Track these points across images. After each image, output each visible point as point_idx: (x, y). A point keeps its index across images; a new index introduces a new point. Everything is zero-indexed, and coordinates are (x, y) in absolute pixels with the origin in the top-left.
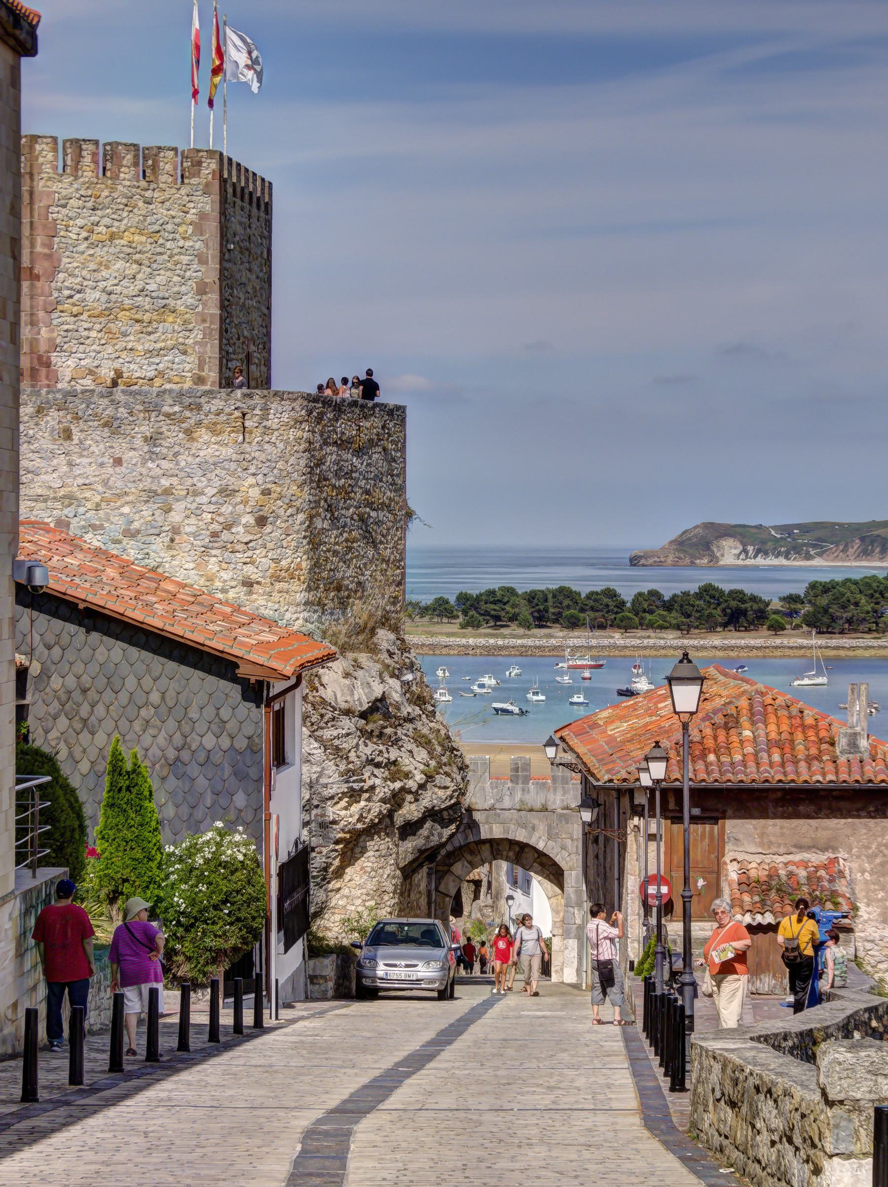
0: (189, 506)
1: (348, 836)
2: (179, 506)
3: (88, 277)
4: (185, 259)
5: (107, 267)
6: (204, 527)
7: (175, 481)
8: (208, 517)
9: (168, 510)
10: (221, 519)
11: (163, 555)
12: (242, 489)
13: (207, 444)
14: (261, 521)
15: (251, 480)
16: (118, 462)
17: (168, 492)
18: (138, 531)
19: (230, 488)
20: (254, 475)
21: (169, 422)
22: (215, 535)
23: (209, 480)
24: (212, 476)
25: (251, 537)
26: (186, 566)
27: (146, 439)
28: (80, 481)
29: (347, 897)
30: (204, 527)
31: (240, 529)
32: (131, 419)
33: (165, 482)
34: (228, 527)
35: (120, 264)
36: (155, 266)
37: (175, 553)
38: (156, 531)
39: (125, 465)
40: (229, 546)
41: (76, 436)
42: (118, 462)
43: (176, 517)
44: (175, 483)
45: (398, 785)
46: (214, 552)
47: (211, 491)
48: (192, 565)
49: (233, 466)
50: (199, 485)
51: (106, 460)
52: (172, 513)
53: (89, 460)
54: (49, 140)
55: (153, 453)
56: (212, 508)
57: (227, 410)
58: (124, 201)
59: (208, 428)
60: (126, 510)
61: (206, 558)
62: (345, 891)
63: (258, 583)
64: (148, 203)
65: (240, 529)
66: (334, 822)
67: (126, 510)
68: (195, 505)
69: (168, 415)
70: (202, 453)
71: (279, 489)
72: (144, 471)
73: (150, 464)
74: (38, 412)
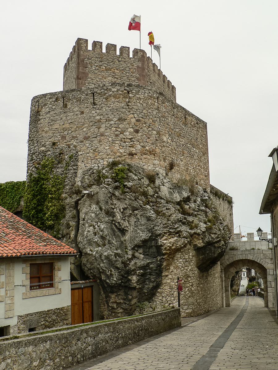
0: (107, 125)
1: (168, 252)
2: (103, 126)
3: (99, 80)
4: (133, 79)
5: (105, 78)
6: (113, 132)
7: (102, 117)
8: (114, 129)
9: (99, 128)
10: (119, 130)
11: (97, 145)
12: (128, 119)
13: (114, 103)
14: (137, 131)
15: (132, 116)
16: (82, 113)
17: (99, 121)
18: (89, 137)
19: (123, 118)
20: (133, 114)
21: (99, 96)
22: (117, 135)
23: (114, 116)
24: (115, 114)
25: (132, 137)
26: (106, 148)
27: (91, 103)
28: (70, 121)
29: (171, 279)
30: (113, 132)
31: (128, 133)
32: (87, 97)
33: (98, 117)
34: (122, 133)
35: (110, 78)
36: (122, 80)
37: (102, 143)
38: (95, 136)
39: (84, 113)
40: (123, 140)
41: (69, 107)
42: (82, 113)
43: (102, 130)
44: (102, 118)
45: (193, 232)
46: (117, 142)
47: (116, 119)
48: (108, 147)
49: (124, 110)
50: (110, 117)
51: (78, 113)
52: (101, 129)
53: (73, 114)
54: (85, 40)
55: (93, 107)
56: (115, 126)
57: (121, 90)
58: (112, 60)
59: (113, 96)
60: (85, 129)
61: (114, 144)
62: (170, 276)
63: (136, 154)
64: (119, 61)
65: (128, 133)
66: (161, 246)
67: (85, 129)
68: (109, 125)
69: (99, 94)
70: (111, 106)
71: (144, 120)
72: (91, 115)
73: (93, 112)
74: (56, 99)
